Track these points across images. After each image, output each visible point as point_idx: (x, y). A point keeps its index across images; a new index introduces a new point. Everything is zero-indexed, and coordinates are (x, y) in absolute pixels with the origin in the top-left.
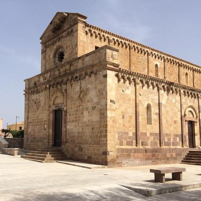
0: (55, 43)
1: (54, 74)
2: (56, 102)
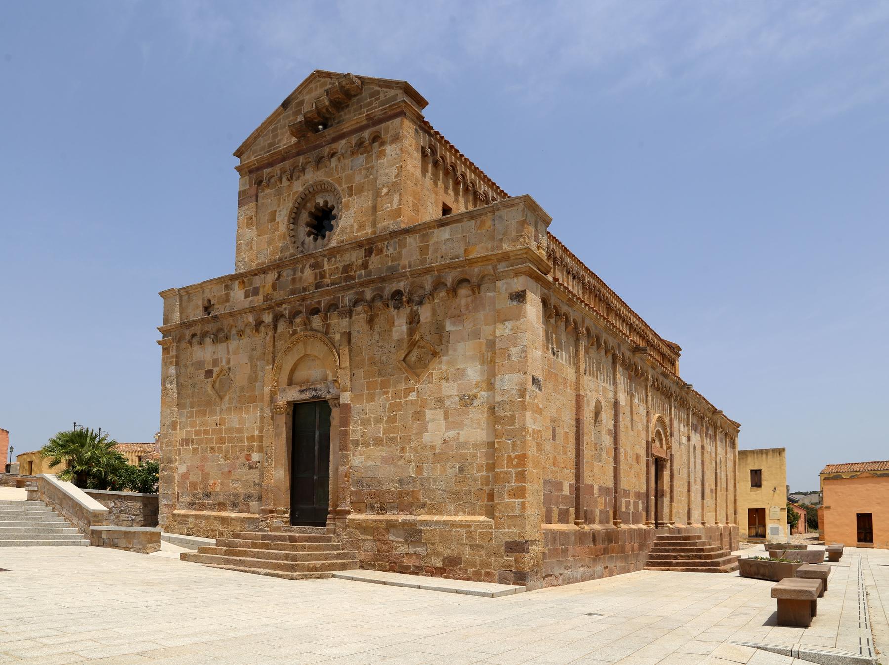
0: (302, 175)
1: (294, 280)
2: (302, 374)
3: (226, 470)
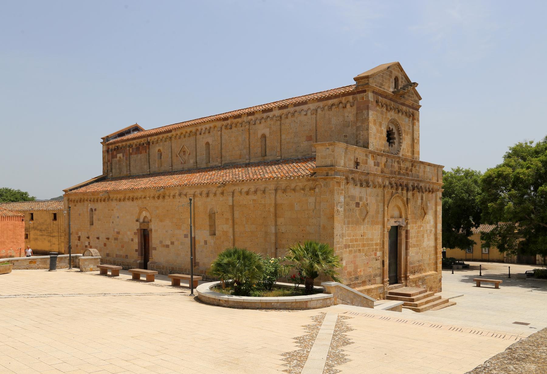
3: (366, 262)
